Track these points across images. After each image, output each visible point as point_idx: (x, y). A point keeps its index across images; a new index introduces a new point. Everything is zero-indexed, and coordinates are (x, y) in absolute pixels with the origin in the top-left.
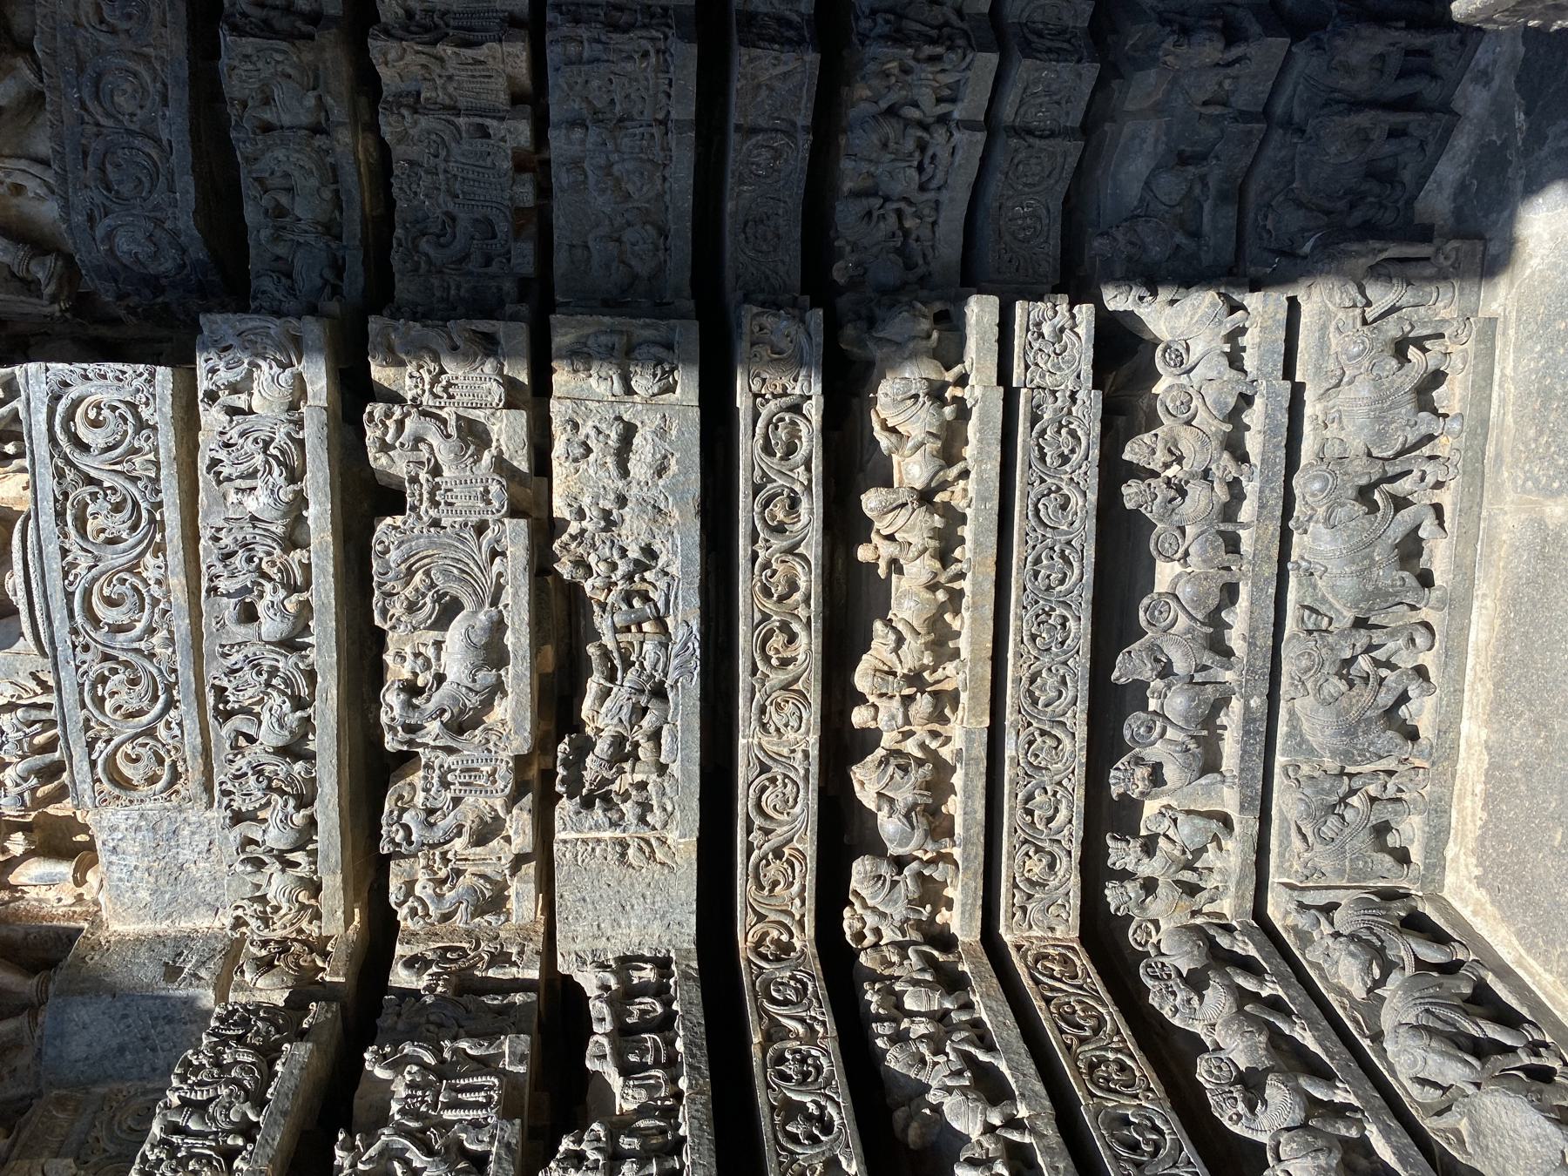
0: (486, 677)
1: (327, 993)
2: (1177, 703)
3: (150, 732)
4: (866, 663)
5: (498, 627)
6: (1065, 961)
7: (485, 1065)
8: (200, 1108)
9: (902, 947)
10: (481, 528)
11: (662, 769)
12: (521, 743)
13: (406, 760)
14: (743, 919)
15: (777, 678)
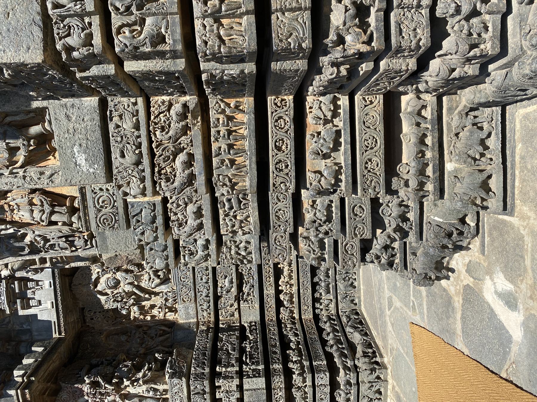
0: (231, 285)
1: (211, 328)
2: (323, 284)
3: (188, 294)
4: (281, 281)
5: (232, 279)
6: (310, 320)
7: (233, 335)
8: (201, 340)
9: (288, 319)
10: (230, 266)
11: (254, 296)
12: (236, 294)
13: (221, 297)
14: (266, 316)
15: (268, 283)
